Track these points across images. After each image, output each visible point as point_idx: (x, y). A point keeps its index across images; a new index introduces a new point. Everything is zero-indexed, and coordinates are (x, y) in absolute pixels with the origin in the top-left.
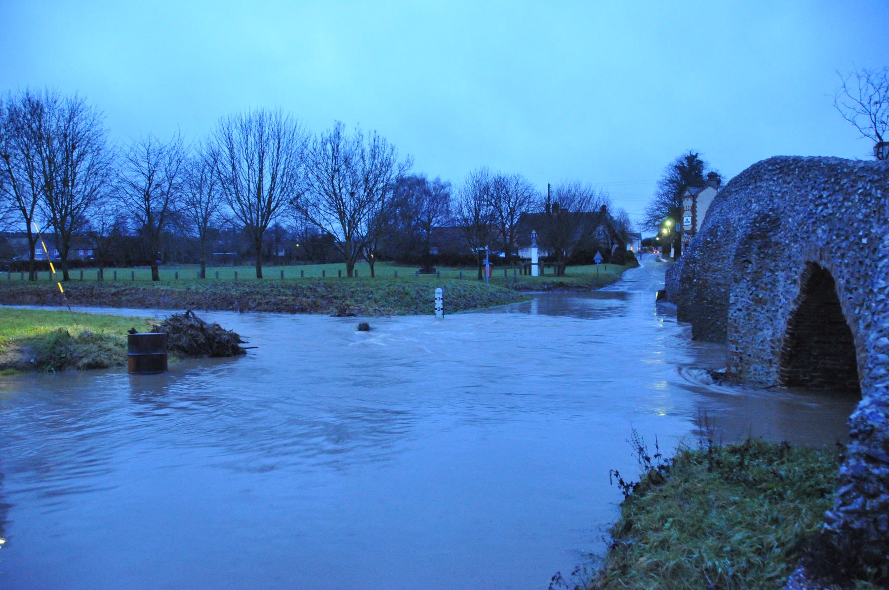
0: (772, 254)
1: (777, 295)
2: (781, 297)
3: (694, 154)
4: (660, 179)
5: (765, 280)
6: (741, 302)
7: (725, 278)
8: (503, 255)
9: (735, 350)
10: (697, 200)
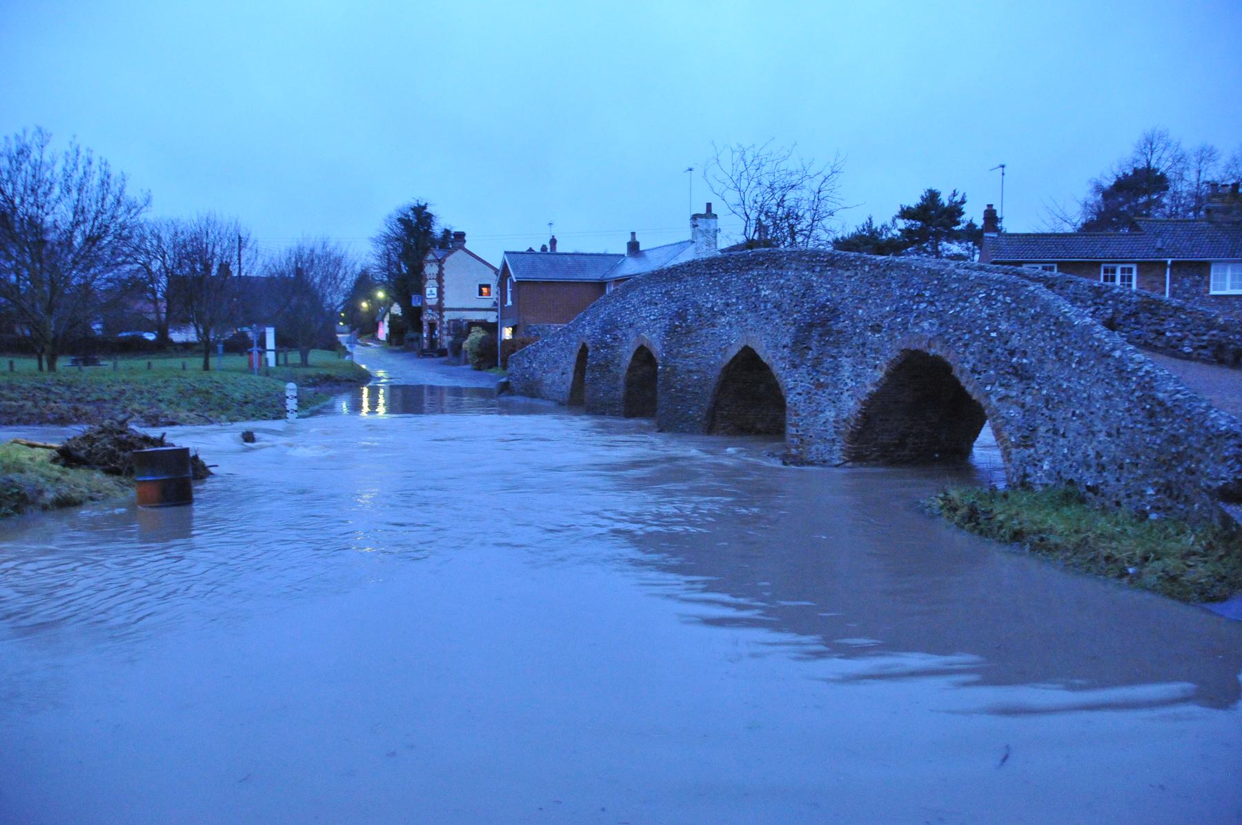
0: (834, 342)
1: (839, 380)
2: (848, 381)
3: (423, 204)
4: (374, 233)
5: (826, 365)
6: (801, 386)
7: (698, 364)
8: (151, 337)
9: (795, 433)
10: (444, 266)
